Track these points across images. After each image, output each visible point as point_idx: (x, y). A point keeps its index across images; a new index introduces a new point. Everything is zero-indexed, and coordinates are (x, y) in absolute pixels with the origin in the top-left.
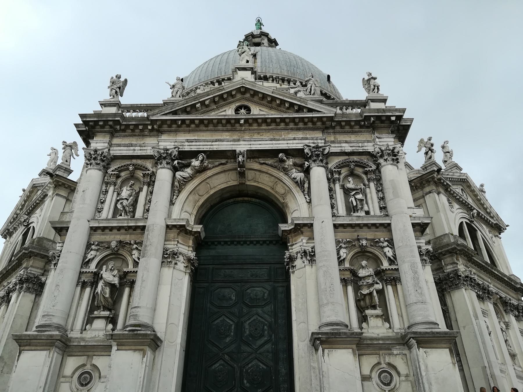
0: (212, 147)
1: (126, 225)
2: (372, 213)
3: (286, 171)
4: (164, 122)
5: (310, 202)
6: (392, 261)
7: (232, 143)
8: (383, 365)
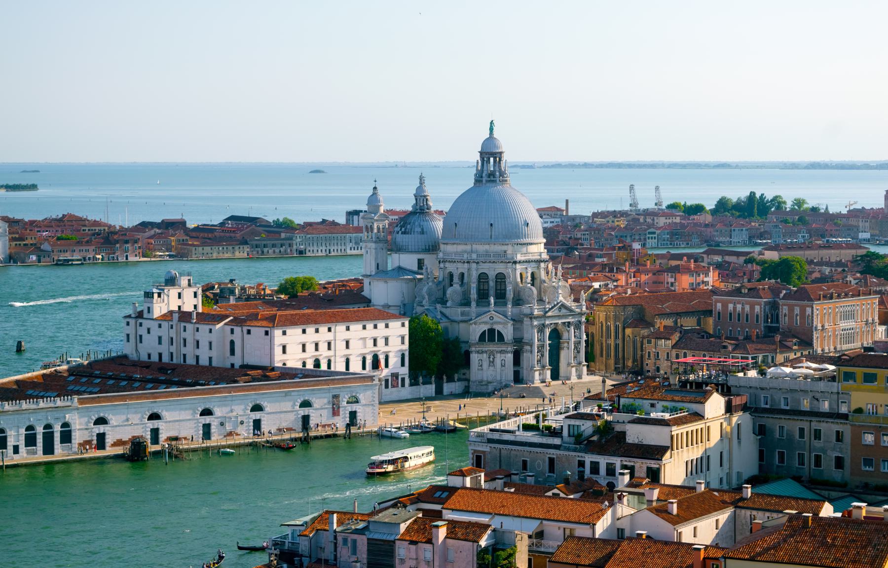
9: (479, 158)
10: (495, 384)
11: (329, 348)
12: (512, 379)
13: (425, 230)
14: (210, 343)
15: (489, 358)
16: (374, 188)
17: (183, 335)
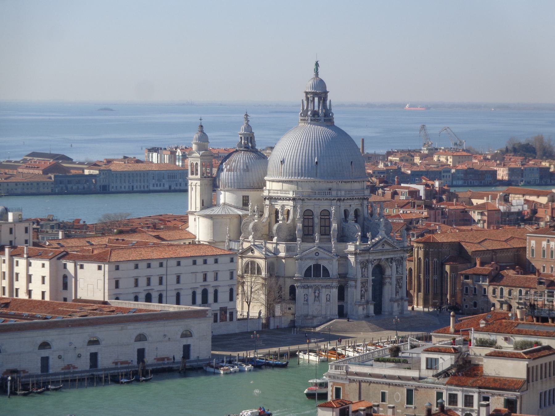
3: (388, 262)
6: (401, 284)
9: (304, 99)
10: (320, 318)
11: (161, 283)
12: (337, 313)
13: (249, 168)
14: (43, 278)
15: (315, 292)
17: (16, 270)
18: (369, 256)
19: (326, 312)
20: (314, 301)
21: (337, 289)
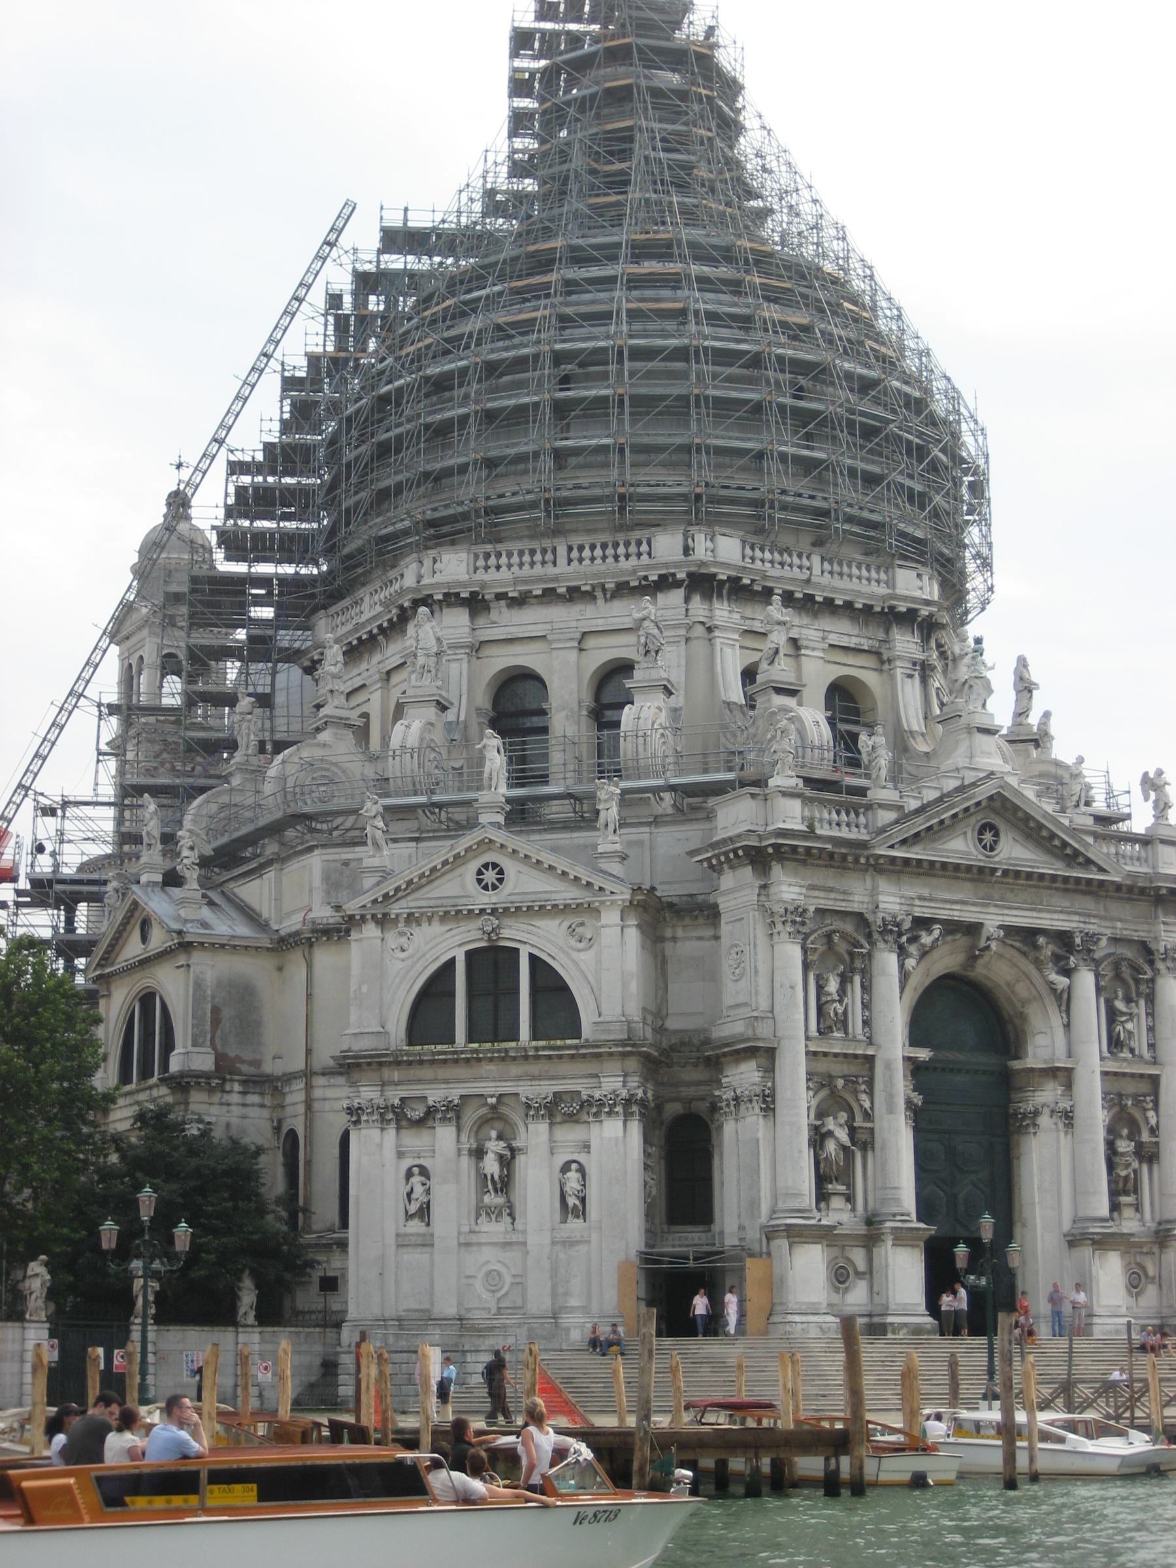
0: (951, 913)
1: (851, 1052)
2: (1137, 1052)
3: (1038, 964)
4: (893, 859)
5: (1067, 1026)
6: (1154, 1131)
7: (978, 909)
8: (1133, 1266)
15: (479, 1153)
16: (170, 495)
18: (874, 892)
19: (554, 1295)
20: (478, 1216)
21: (635, 1127)
